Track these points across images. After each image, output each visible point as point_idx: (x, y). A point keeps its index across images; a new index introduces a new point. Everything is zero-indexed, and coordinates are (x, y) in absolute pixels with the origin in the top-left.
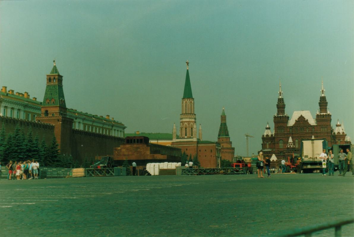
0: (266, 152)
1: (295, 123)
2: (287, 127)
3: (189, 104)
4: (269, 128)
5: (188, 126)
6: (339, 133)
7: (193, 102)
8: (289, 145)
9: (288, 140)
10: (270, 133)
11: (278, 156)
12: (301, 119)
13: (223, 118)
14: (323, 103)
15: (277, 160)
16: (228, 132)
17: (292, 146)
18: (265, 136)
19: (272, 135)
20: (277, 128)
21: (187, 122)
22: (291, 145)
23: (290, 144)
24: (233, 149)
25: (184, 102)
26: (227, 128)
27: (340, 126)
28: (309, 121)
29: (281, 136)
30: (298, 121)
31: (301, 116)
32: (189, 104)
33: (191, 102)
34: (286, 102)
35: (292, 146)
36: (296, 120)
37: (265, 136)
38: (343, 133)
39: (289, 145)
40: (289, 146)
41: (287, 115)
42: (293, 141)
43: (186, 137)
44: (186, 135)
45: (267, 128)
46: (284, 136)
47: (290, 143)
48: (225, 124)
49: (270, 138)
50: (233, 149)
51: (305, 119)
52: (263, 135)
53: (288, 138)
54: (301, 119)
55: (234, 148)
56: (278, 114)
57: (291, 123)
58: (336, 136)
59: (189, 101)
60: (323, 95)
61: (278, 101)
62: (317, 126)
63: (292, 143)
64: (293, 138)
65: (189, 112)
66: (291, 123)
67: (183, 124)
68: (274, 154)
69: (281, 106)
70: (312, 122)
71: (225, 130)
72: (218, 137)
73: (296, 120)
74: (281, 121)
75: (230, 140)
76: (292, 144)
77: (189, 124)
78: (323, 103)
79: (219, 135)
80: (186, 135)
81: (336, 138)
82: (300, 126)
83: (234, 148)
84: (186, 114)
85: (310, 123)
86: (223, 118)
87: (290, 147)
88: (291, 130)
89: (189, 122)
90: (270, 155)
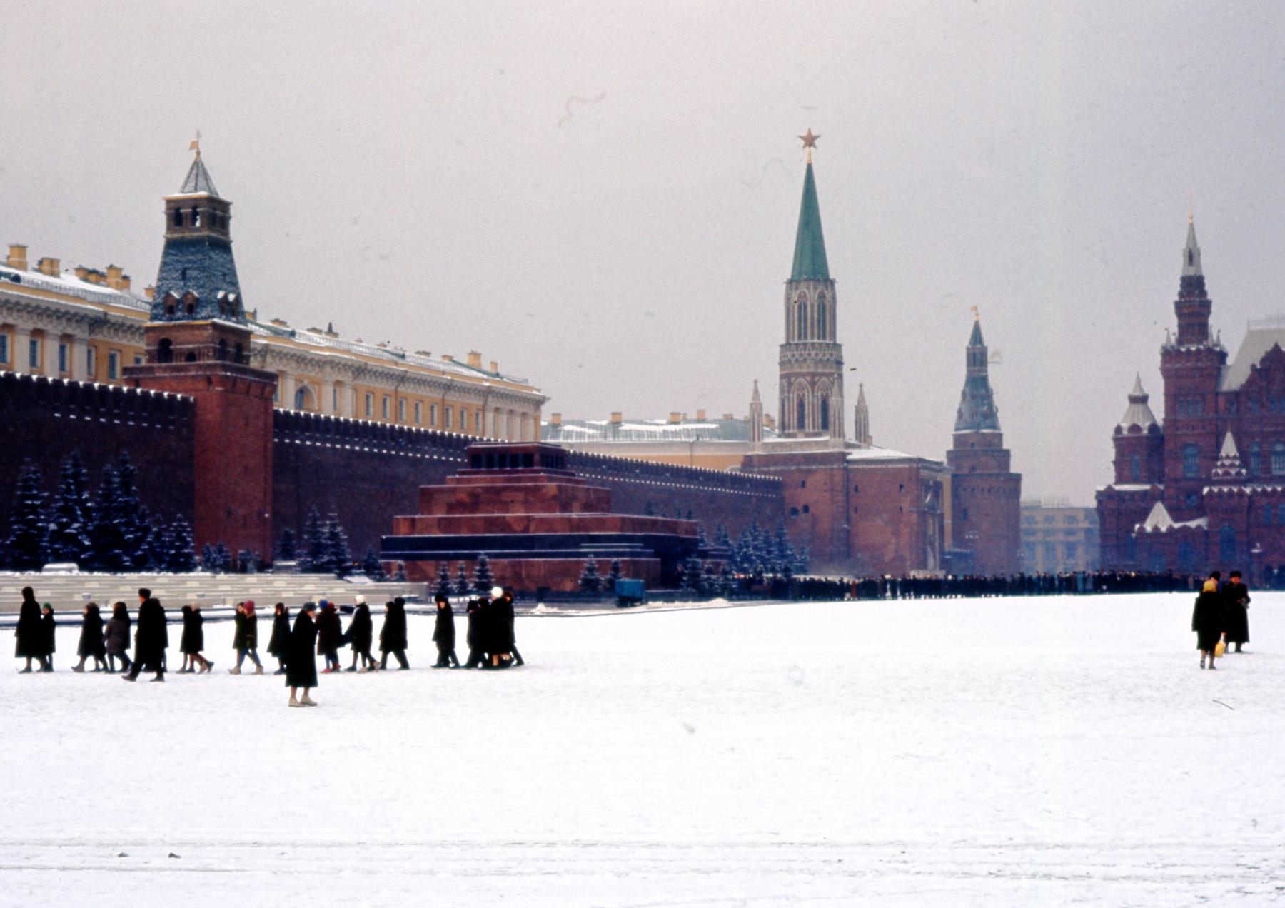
1: (1250, 382)
7: (828, 295)
9: (1219, 446)
17: (1233, 472)
18: (1125, 433)
21: (803, 375)
22: (1232, 466)
23: (1227, 462)
32: (812, 306)
33: (822, 296)
36: (1253, 367)
37: (1125, 433)
42: (1239, 449)
47: (1228, 457)
56: (1180, 341)
63: (1235, 457)
67: (790, 384)
69: (1193, 304)
77: (813, 384)
89: (813, 375)
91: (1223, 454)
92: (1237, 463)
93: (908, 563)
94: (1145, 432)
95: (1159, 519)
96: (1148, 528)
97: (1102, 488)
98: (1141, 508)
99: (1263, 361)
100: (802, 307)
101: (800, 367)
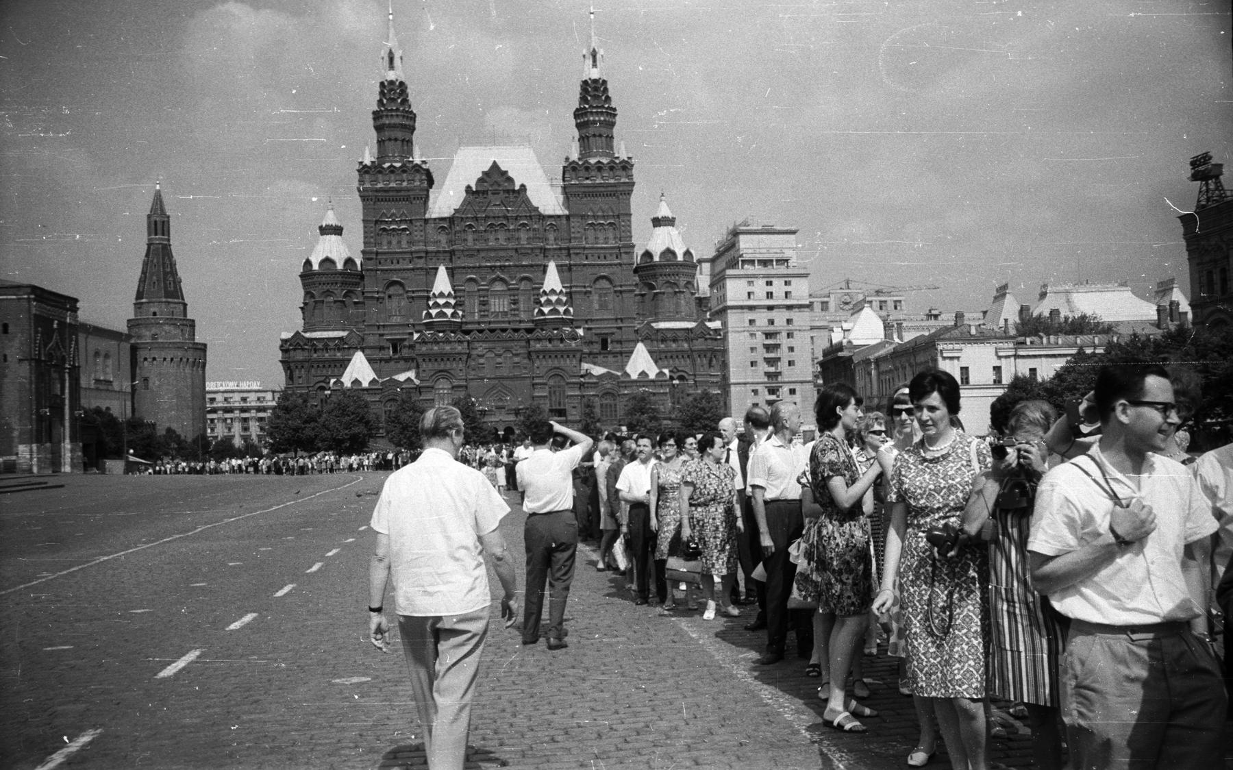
0: (320, 346)
2: (426, 221)
4: (337, 231)
6: (669, 253)
8: (436, 305)
9: (430, 284)
10: (337, 250)
11: (381, 360)
12: (495, 183)
13: (159, 224)
14: (595, 108)
15: (373, 382)
16: (177, 282)
17: (449, 311)
18: (316, 267)
19: (349, 261)
20: (374, 227)
22: (447, 305)
24: (203, 348)
26: (173, 265)
27: (669, 222)
28: (528, 193)
29: (397, 267)
30: (477, 192)
34: (417, 103)
35: (449, 311)
36: (468, 188)
37: (316, 267)
38: (687, 253)
39: (436, 305)
41: (424, 162)
42: (453, 287)
45: (325, 230)
46: (411, 266)
47: (441, 295)
48: (166, 250)
49: (340, 274)
50: (203, 348)
51: (510, 180)
52: (308, 263)
54: (495, 183)
55: (205, 345)
57: (445, 200)
58: (655, 266)
60: (595, 74)
61: (382, 93)
62: (568, 217)
64: (451, 273)
66: (445, 200)
68: (363, 350)
69: (394, 114)
70: (547, 198)
71: (166, 274)
73: (468, 188)
74: (392, 186)
75: (185, 314)
76: (453, 302)
78: (595, 108)
79: (139, 295)
81: (654, 276)
82: (487, 217)
83: (205, 345)
85: (535, 204)
86: (159, 224)
87: (442, 314)
88: (443, 238)
91: (436, 290)
92: (453, 302)
93: (16, 434)
94: (340, 266)
95: (359, 370)
96: (347, 380)
97: (287, 335)
99: (480, 181)
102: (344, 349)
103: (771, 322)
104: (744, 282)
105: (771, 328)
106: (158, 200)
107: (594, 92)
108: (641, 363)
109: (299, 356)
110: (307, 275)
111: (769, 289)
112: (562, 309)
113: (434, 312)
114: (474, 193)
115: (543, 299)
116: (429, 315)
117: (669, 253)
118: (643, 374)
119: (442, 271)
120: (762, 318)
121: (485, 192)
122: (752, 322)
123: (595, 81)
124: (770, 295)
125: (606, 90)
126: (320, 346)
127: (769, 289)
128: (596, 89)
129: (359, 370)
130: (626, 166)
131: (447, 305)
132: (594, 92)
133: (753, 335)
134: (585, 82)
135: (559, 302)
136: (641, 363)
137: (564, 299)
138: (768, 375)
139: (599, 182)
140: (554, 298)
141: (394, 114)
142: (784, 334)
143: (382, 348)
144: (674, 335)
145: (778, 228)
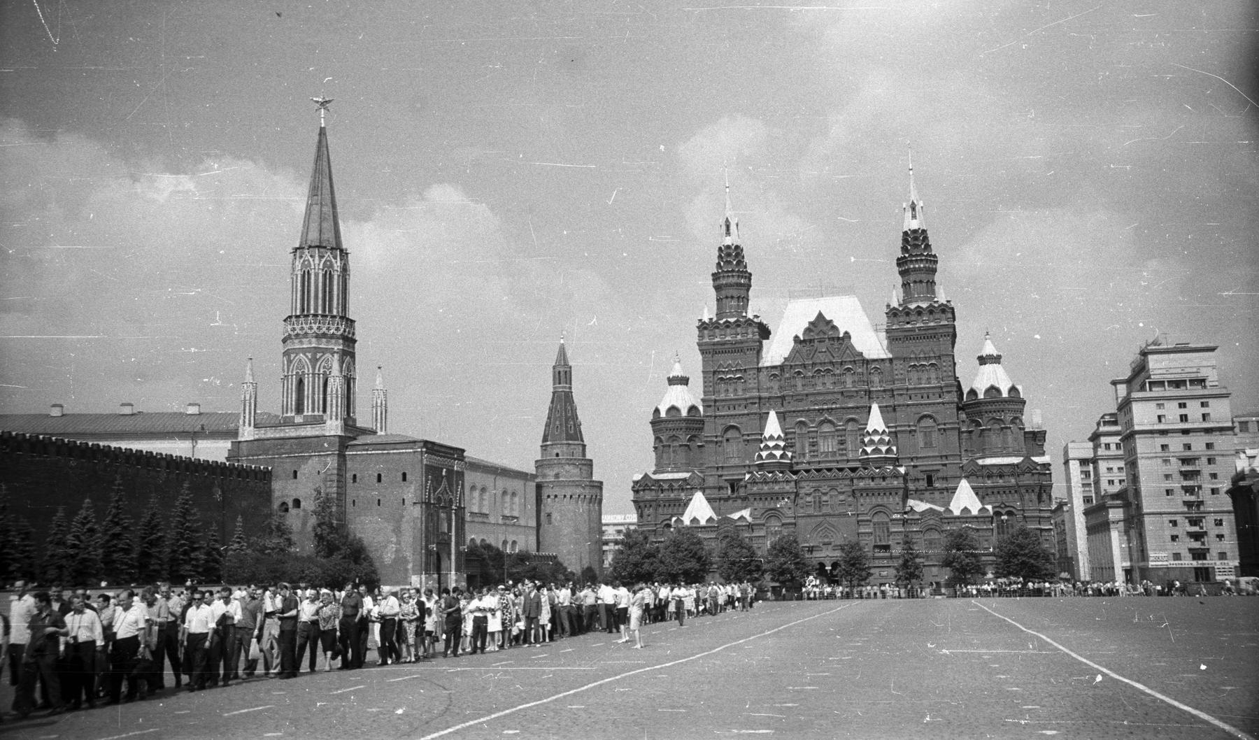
0: (666, 486)
1: (795, 352)
2: (759, 370)
3: (317, 275)
4: (684, 381)
5: (308, 369)
6: (993, 390)
8: (767, 447)
9: (762, 428)
10: (684, 399)
11: (720, 499)
12: (821, 332)
13: (563, 374)
14: (916, 256)
15: (710, 520)
16: (577, 426)
18: (663, 414)
19: (693, 409)
20: (713, 377)
21: (304, 351)
22: (776, 447)
23: (771, 444)
24: (599, 486)
25: (298, 264)
26: (574, 410)
27: (996, 359)
28: (853, 341)
29: (733, 412)
30: (804, 341)
31: (820, 315)
32: (317, 275)
33: (328, 267)
35: (778, 453)
36: (796, 337)
37: (663, 414)
38: (1013, 389)
39: (767, 447)
40: (764, 454)
41: (756, 317)
43: (299, 419)
44: (299, 409)
45: (673, 381)
47: (771, 438)
48: (568, 397)
49: (685, 420)
51: (835, 328)
52: (657, 411)
53: (763, 417)
54: (821, 332)
55: (601, 483)
57: (776, 351)
58: (979, 403)
59: (317, 261)
60: (915, 225)
61: (720, 257)
62: (891, 360)
63: (779, 437)
64: (782, 417)
65: (316, 310)
66: (776, 351)
67: (290, 362)
68: (703, 490)
69: (732, 274)
70: (871, 342)
72: (540, 443)
73: (796, 337)
74: (730, 340)
75: (584, 455)
76: (782, 444)
77: (314, 361)
78: (916, 256)
79: (545, 439)
80: (299, 409)
81: (980, 414)
82: (814, 364)
83: (601, 483)
84: (302, 319)
85: (859, 348)
86: (563, 374)
87: (771, 456)
88: (775, 385)
90: (683, 496)
92: (782, 444)
93: (410, 566)
94: (684, 413)
95: (699, 509)
96: (686, 520)
97: (638, 477)
98: (675, 498)
99: (808, 330)
100: (306, 276)
101: (301, 342)
102: (687, 487)
103: (1188, 447)
104: (1153, 404)
105: (1188, 453)
106: (562, 352)
107: (915, 243)
108: (965, 499)
109: (648, 496)
110: (656, 423)
111: (1183, 411)
112: (884, 448)
113: (764, 454)
114: (801, 342)
115: (866, 440)
116: (760, 457)
117: (993, 390)
118: (966, 510)
119: (773, 416)
120: (1176, 444)
121: (811, 341)
122: (1164, 447)
123: (915, 231)
124: (1184, 418)
125: (926, 238)
126: (666, 486)
127: (1183, 411)
128: (916, 239)
129: (699, 509)
130: (947, 310)
131: (776, 447)
132: (915, 243)
133: (1166, 461)
134: (905, 233)
135: (881, 441)
136: (965, 499)
137: (887, 439)
138: (1188, 504)
139: (923, 327)
140: (876, 438)
141: (732, 274)
142: (1204, 460)
143: (720, 488)
144: (1001, 471)
145: (1192, 346)
